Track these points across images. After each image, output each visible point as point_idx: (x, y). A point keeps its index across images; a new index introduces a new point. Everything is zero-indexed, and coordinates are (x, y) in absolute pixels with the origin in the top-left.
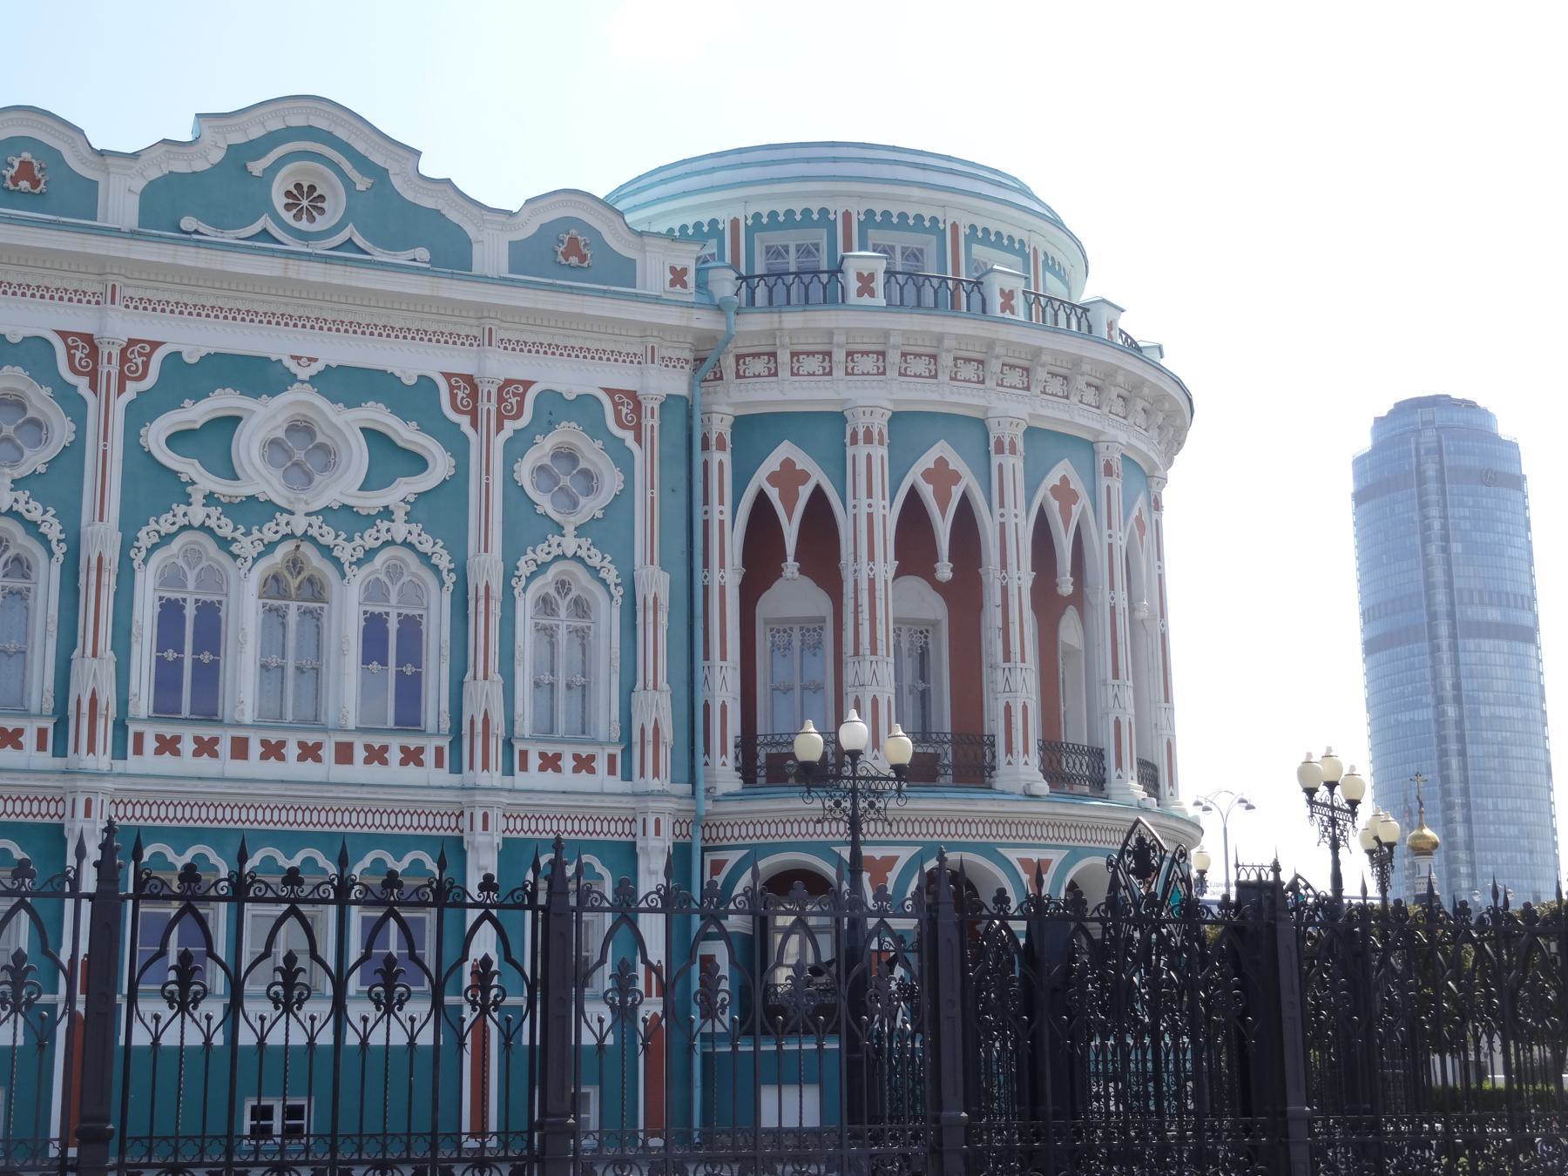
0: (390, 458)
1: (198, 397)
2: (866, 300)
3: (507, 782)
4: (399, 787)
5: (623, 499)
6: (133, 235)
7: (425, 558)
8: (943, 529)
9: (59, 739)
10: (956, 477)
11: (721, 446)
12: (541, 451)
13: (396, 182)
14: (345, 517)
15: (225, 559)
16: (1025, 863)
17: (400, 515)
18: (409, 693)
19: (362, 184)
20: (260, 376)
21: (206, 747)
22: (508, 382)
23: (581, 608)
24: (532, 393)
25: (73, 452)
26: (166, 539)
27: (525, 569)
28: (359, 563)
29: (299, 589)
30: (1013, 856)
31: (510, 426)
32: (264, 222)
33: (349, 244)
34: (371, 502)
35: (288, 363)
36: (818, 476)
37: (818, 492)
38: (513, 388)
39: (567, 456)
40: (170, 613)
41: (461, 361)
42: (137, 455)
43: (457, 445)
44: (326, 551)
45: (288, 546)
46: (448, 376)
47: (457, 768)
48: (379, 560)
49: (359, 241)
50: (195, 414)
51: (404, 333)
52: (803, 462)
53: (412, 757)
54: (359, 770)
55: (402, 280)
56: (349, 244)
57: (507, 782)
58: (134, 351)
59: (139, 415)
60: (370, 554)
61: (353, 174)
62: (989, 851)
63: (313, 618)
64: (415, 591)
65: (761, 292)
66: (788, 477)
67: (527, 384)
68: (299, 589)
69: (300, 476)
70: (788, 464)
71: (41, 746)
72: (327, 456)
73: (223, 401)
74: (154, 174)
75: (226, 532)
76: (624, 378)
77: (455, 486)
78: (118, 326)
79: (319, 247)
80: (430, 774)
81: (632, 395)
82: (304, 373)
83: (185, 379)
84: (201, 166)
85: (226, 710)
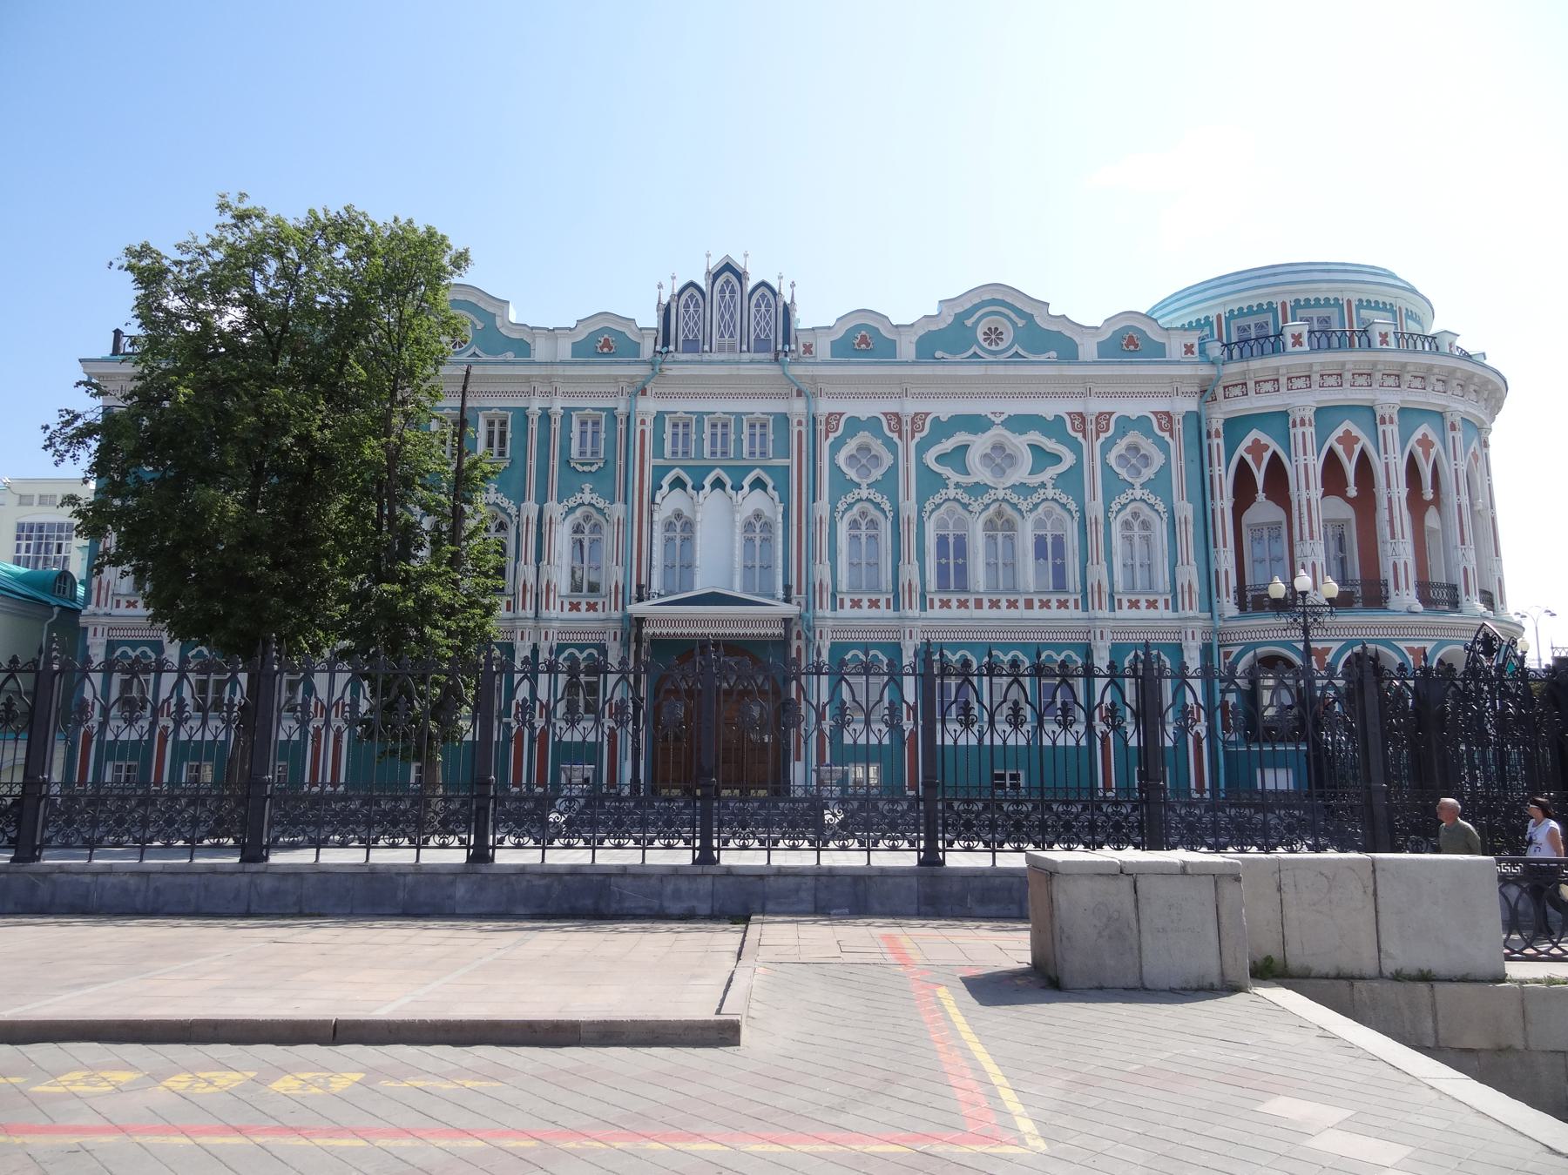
0: (1043, 458)
2: (1298, 348)
3: (1112, 615)
4: (1056, 620)
5: (1166, 466)
6: (914, 363)
7: (1063, 506)
8: (1350, 469)
9: (896, 603)
10: (1357, 440)
11: (1218, 435)
12: (1121, 447)
13: (1038, 320)
14: (1023, 489)
15: (966, 514)
16: (1411, 650)
17: (1049, 486)
18: (1059, 573)
19: (1021, 323)
20: (977, 424)
21: (963, 604)
22: (1101, 414)
23: (1145, 525)
24: (1114, 418)
25: (894, 468)
26: (938, 506)
27: (1115, 507)
28: (1031, 511)
29: (1001, 526)
30: (1402, 645)
32: (975, 349)
33: (1016, 354)
34: (1035, 480)
35: (992, 417)
36: (1274, 446)
37: (1275, 456)
38: (1104, 417)
39: (1134, 448)
40: (942, 541)
41: (1076, 406)
42: (923, 468)
44: (1014, 506)
45: (996, 505)
46: (1069, 414)
47: (1086, 609)
48: (1040, 509)
49: (1021, 352)
50: (948, 445)
51: (1046, 395)
52: (1265, 439)
53: (1063, 604)
54: (1037, 612)
55: (1044, 369)
56: (1016, 354)
57: (1112, 615)
58: (918, 417)
59: (922, 448)
60: (1036, 506)
61: (1016, 319)
62: (1387, 643)
65: (1236, 352)
66: (1257, 449)
67: (1111, 414)
68: (1001, 526)
69: (1000, 471)
70: (1256, 441)
71: (888, 607)
72: (1011, 459)
73: (961, 438)
74: (922, 332)
75: (966, 501)
76: (1162, 405)
77: (1077, 468)
78: (910, 407)
79: (1001, 358)
80: (1072, 612)
81: (1167, 414)
82: (998, 421)
83: (943, 428)
84: (943, 326)
85: (971, 586)
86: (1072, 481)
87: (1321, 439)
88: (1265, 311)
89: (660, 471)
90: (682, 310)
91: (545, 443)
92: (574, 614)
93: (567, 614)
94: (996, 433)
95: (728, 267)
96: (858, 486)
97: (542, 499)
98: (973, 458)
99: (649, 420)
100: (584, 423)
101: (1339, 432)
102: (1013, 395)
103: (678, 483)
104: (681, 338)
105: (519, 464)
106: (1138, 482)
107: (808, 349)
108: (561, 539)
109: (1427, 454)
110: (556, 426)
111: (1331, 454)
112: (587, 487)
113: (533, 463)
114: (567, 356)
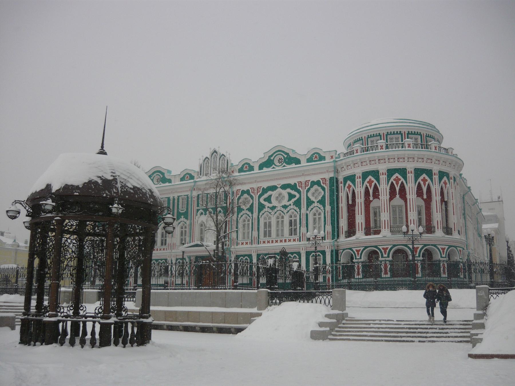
0: (291, 196)
1: (266, 192)
5: (324, 197)
7: (295, 210)
10: (373, 181)
11: (341, 183)
12: (312, 190)
14: (285, 207)
16: (383, 249)
17: (292, 205)
19: (286, 156)
30: (380, 247)
32: (273, 166)
34: (287, 204)
36: (353, 186)
39: (316, 190)
40: (265, 223)
43: (299, 192)
44: (282, 212)
48: (290, 212)
50: (266, 196)
52: (351, 184)
62: (376, 247)
63: (282, 221)
64: (295, 216)
73: (270, 193)
82: (279, 187)
83: (265, 191)
84: (266, 160)
86: (298, 203)
88: (360, 140)
89: (198, 210)
94: (279, 190)
95: (215, 152)
96: (244, 210)
98: (273, 199)
100: (183, 199)
102: (281, 179)
103: (202, 214)
106: (316, 201)
109: (397, 184)
110: (176, 201)
112: (182, 216)
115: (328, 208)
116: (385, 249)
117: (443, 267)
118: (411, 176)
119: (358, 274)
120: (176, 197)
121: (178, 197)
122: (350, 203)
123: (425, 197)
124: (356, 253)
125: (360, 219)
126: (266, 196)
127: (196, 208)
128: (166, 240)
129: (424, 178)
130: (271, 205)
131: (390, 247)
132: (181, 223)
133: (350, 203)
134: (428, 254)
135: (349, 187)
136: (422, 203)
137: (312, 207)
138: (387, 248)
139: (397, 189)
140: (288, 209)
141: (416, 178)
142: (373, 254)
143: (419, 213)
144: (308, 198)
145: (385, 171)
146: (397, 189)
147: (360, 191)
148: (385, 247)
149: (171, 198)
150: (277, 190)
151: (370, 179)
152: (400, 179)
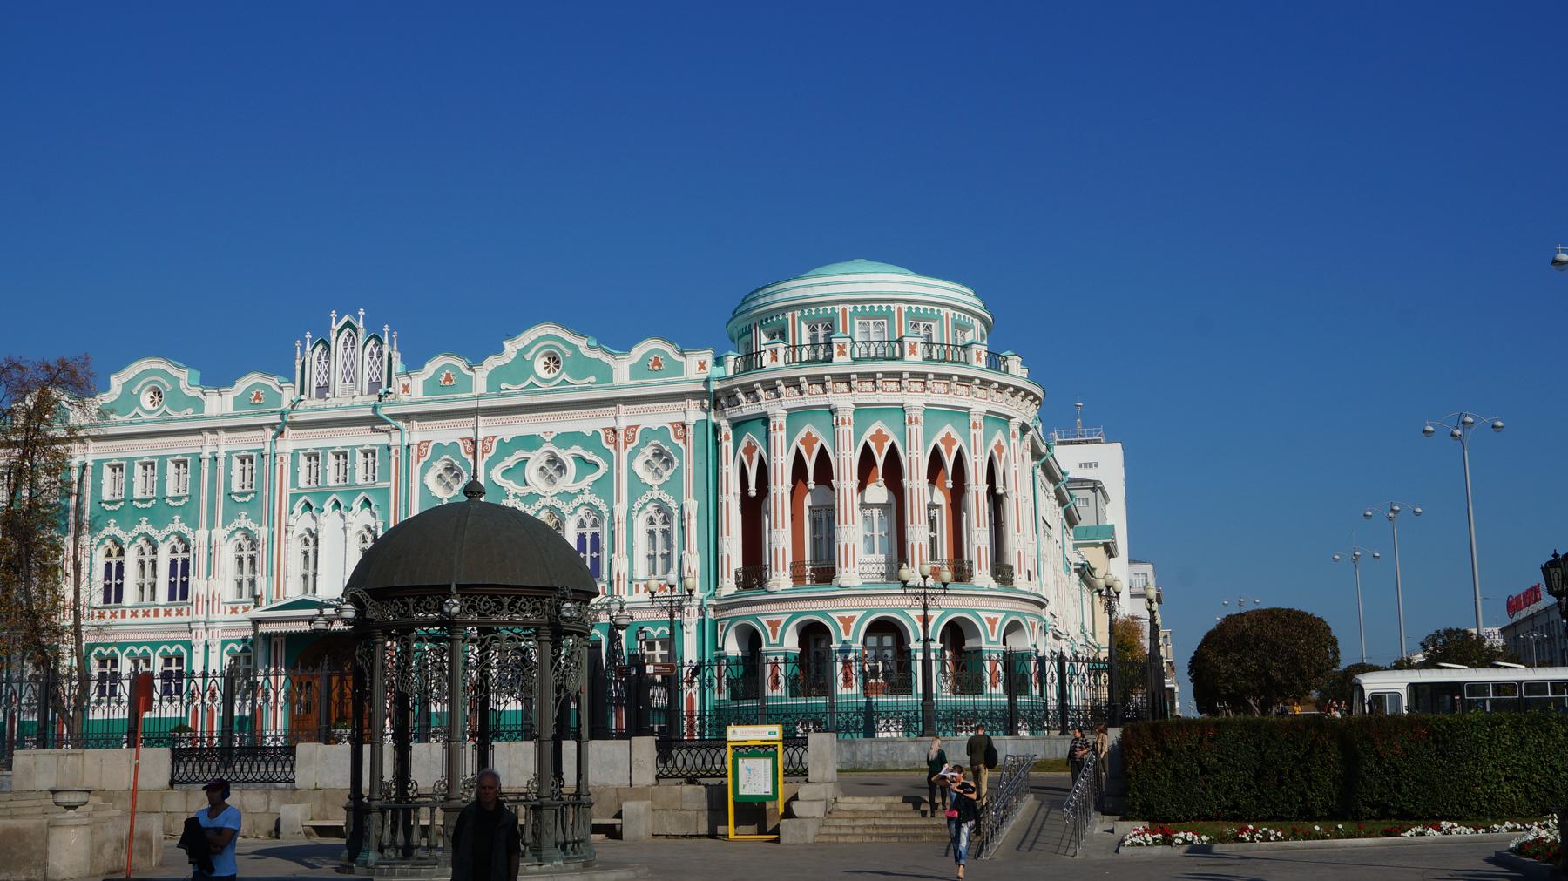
11: (727, 438)
14: (566, 496)
16: (842, 619)
20: (531, 442)
30: (835, 616)
31: (630, 447)
32: (532, 379)
34: (574, 488)
36: (761, 448)
43: (608, 457)
50: (510, 462)
77: (608, 477)
83: (506, 448)
86: (604, 487)
87: (790, 439)
90: (315, 362)
91: (213, 480)
92: (234, 617)
93: (229, 617)
97: (211, 526)
98: (532, 472)
99: (287, 459)
101: (802, 434)
104: (314, 385)
105: (194, 498)
107: (406, 388)
108: (227, 555)
111: (798, 451)
113: (205, 498)
114: (229, 409)
115: (692, 506)
116: (847, 622)
117: (992, 668)
118: (917, 430)
119: (776, 683)
120: (222, 453)
121: (229, 453)
122: (753, 492)
123: (949, 484)
124: (769, 629)
125: (779, 539)
126: (510, 462)
127: (288, 490)
128: (185, 585)
129: (948, 435)
130: (523, 491)
131: (859, 615)
132: (238, 535)
133: (753, 492)
134: (956, 632)
135: (750, 450)
136: (940, 498)
137: (644, 499)
138: (852, 619)
139: (880, 462)
140: (575, 503)
141: (928, 436)
142: (813, 633)
143: (932, 523)
144: (632, 474)
145: (849, 415)
146: (880, 462)
147: (782, 466)
148: (847, 615)
149: (206, 453)
150: (542, 450)
151: (809, 434)
152: (887, 438)
